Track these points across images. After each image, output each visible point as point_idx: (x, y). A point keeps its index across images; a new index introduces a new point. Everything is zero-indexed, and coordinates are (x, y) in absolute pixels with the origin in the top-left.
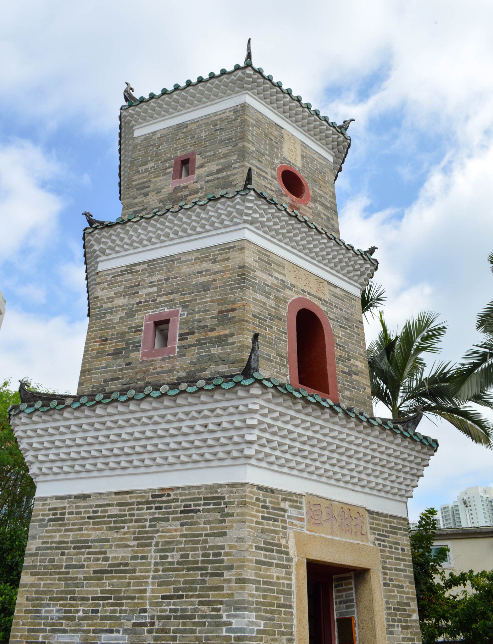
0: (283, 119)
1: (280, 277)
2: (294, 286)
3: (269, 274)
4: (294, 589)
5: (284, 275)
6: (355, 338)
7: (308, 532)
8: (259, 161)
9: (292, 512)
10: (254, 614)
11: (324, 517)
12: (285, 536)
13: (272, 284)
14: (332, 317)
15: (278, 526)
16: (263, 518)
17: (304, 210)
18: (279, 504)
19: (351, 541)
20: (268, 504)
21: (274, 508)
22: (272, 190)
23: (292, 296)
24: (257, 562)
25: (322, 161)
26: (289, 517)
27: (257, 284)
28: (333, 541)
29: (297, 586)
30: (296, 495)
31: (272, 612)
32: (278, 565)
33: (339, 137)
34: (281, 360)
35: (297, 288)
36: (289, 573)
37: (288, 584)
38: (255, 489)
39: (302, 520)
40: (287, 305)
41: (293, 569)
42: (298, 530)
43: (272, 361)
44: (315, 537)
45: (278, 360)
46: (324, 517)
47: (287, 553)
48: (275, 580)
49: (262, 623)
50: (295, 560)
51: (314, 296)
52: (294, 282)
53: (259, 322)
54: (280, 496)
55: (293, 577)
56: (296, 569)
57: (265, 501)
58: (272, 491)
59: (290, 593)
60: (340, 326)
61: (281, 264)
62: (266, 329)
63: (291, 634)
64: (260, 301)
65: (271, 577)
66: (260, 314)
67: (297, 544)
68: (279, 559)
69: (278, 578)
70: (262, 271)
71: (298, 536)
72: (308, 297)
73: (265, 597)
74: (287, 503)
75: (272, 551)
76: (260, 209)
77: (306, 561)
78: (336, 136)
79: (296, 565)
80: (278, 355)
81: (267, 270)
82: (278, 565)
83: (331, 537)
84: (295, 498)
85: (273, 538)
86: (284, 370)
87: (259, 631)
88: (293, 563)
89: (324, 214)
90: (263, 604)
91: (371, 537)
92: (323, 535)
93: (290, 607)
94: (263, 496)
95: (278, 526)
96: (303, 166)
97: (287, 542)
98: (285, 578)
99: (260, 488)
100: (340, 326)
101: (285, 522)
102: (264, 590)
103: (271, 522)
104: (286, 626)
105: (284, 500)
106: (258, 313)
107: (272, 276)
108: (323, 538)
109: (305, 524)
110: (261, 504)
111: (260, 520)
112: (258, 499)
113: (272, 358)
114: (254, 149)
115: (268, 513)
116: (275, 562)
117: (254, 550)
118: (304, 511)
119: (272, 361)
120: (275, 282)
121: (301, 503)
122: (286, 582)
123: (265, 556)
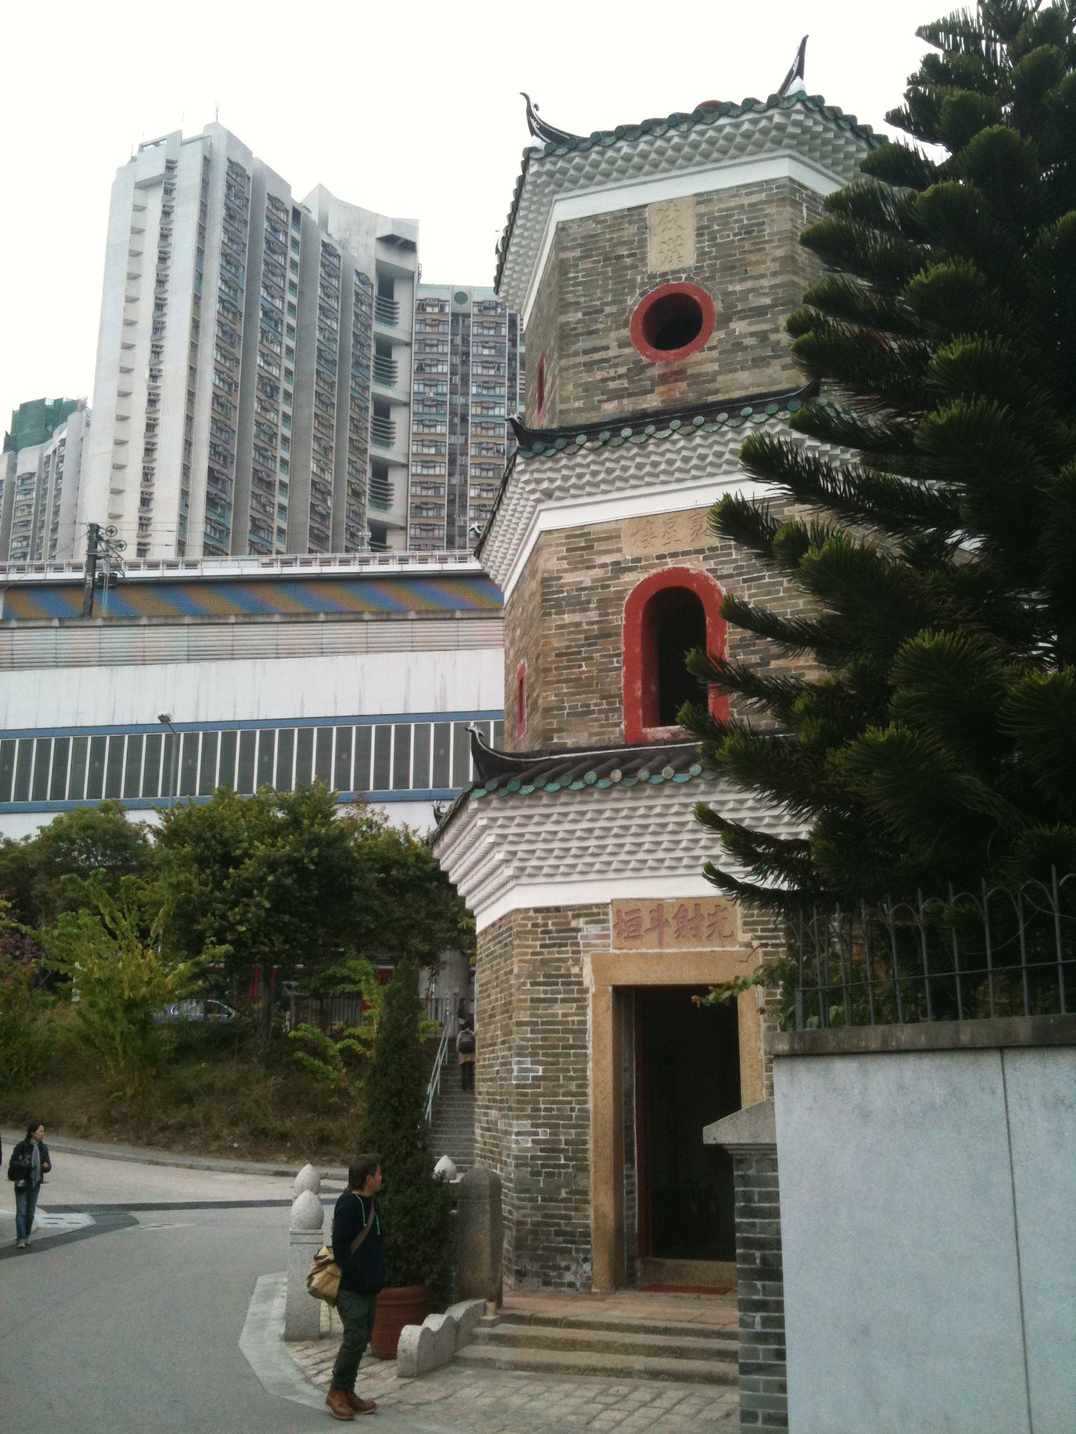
0: (645, 183)
1: (608, 559)
2: (638, 560)
3: (588, 568)
4: (589, 1025)
5: (619, 550)
6: (785, 585)
7: (617, 951)
8: (591, 333)
9: (593, 930)
10: (529, 1059)
11: (647, 924)
12: (577, 962)
13: (594, 581)
14: (725, 572)
15: (567, 952)
16: (542, 946)
17: (696, 363)
18: (569, 923)
19: (699, 949)
20: (551, 927)
21: (558, 931)
22: (620, 377)
23: (634, 579)
24: (532, 1000)
25: (754, 199)
26: (586, 937)
27: (563, 598)
28: (660, 955)
29: (594, 1022)
30: (597, 906)
31: (554, 1055)
32: (564, 1000)
33: (770, 119)
34: (609, 704)
35: (647, 558)
36: (584, 1008)
37: (580, 1022)
38: (531, 914)
39: (607, 936)
40: (624, 603)
41: (590, 1002)
42: (599, 951)
43: (593, 712)
44: (627, 955)
45: (605, 706)
46: (647, 924)
47: (581, 983)
48: (560, 1018)
49: (541, 1068)
50: (593, 990)
51: (685, 553)
52: (638, 552)
53: (568, 661)
54: (570, 913)
55: (589, 1012)
56: (594, 1001)
57: (546, 925)
58: (557, 909)
59: (584, 1032)
60: (745, 581)
61: (611, 534)
62: (581, 666)
63: (585, 1078)
64: (571, 624)
65: (556, 1015)
66: (570, 647)
67: (596, 970)
68: (566, 992)
69: (564, 1015)
70: (572, 570)
71: (596, 960)
72: (670, 564)
73: (544, 1039)
74: (582, 920)
75: (556, 984)
76: (545, 471)
77: (610, 989)
78: (764, 123)
79: (594, 996)
80: (602, 698)
81: (583, 561)
82: (564, 1000)
83: (656, 950)
84: (595, 910)
85: (558, 968)
86: (614, 718)
87: (534, 1078)
88: (590, 995)
89: (752, 334)
90: (542, 1047)
91: (744, 937)
92: (644, 950)
93: (585, 1047)
94: (543, 918)
95: (567, 952)
96: (701, 255)
97: (581, 969)
98: (577, 1015)
99: (537, 910)
100: (745, 581)
101: (577, 944)
102: (544, 1031)
103: (555, 949)
104: (575, 1071)
105: (576, 916)
106: (568, 647)
107: (594, 567)
108: (642, 955)
109: (610, 941)
110: (539, 930)
111: (538, 949)
112: (534, 925)
113: (592, 708)
114: (580, 315)
115: (550, 939)
116: (559, 996)
117: (528, 986)
118: (611, 924)
119: (593, 712)
120: (598, 572)
121: (606, 914)
122: (576, 1018)
123: (545, 992)
